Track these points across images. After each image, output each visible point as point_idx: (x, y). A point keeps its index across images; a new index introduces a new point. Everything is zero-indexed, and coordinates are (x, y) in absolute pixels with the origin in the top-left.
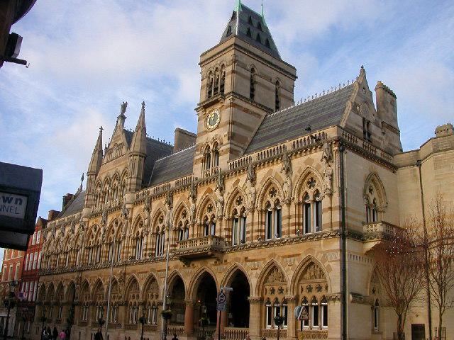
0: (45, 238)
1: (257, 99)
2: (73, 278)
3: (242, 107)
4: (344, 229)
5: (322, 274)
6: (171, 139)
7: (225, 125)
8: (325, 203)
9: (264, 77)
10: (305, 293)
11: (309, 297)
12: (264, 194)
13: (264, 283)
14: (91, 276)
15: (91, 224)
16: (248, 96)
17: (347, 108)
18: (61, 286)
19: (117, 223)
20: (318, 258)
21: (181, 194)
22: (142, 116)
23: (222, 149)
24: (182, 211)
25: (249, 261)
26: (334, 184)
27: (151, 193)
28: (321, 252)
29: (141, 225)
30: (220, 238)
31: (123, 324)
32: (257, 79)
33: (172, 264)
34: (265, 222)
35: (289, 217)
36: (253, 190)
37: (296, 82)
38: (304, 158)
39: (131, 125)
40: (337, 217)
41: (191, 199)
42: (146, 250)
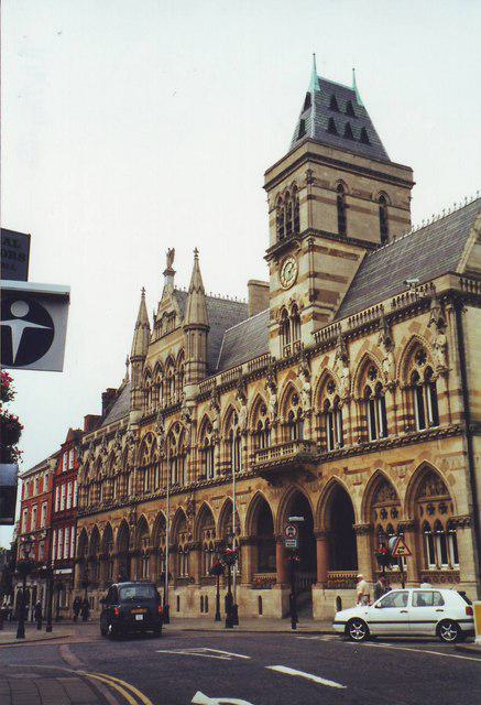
0: (80, 460)
1: (351, 233)
2: (125, 514)
3: (326, 249)
4: (468, 423)
5: (445, 489)
6: (242, 295)
7: (303, 280)
8: (441, 386)
9: (359, 195)
10: (426, 517)
11: (432, 521)
13: (373, 503)
14: (148, 511)
15: (143, 433)
16: (335, 230)
17: (469, 240)
18: (109, 530)
19: (178, 428)
20: (437, 465)
22: (197, 270)
23: (304, 314)
24: (259, 405)
25: (350, 473)
26: (450, 359)
27: (219, 383)
28: (440, 456)
29: (211, 429)
30: (309, 443)
31: (196, 577)
32: (349, 200)
33: (253, 483)
34: (366, 417)
35: (395, 408)
36: (346, 372)
37: (414, 192)
38: (408, 323)
39: (183, 282)
40: (457, 405)
41: (269, 389)
42: (219, 464)
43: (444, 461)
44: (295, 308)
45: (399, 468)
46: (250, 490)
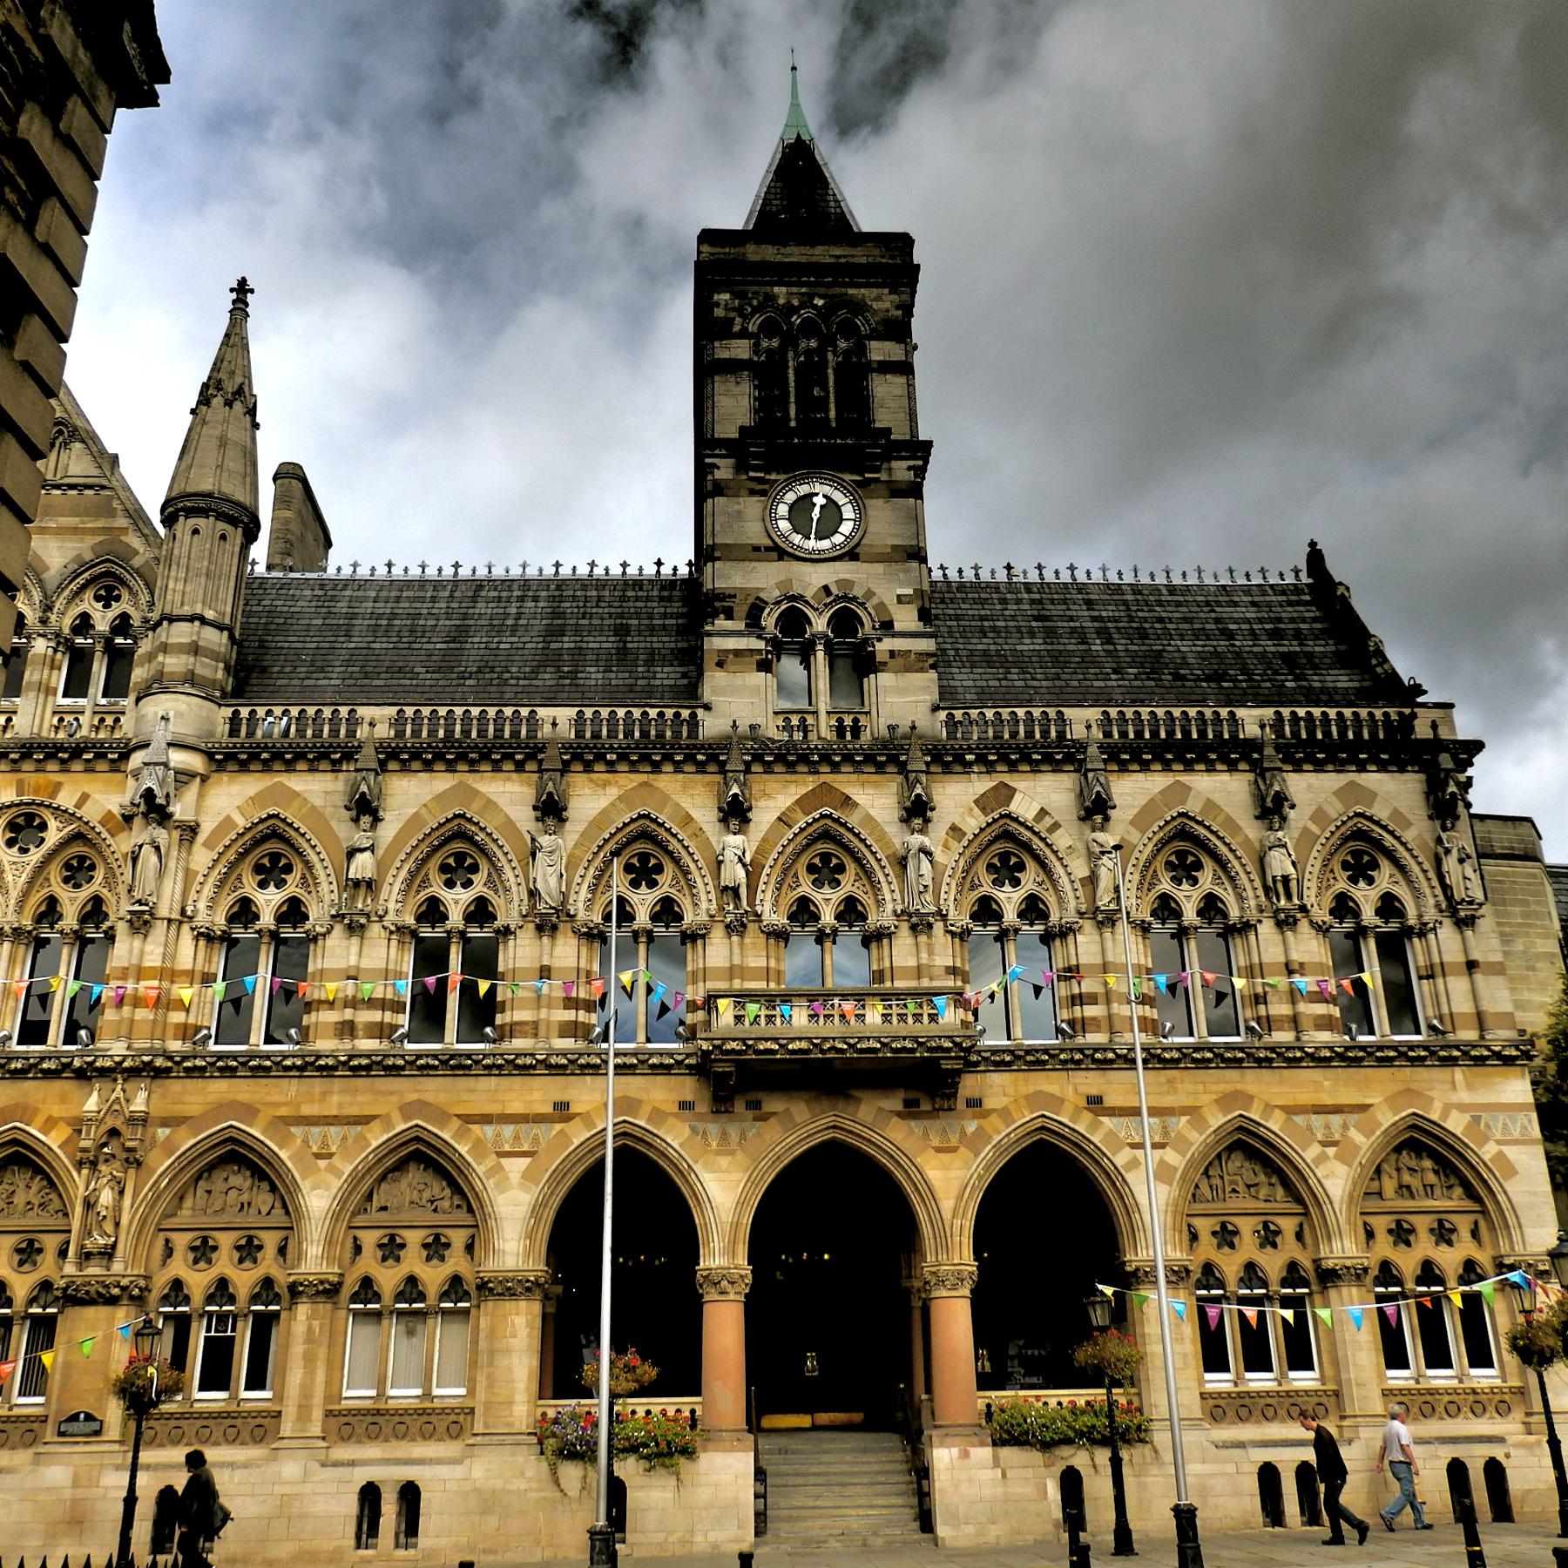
12: (1148, 864)
21: (628, 781)
28: (1462, 1108)
33: (584, 1093)
43: (1476, 1119)
44: (845, 621)
45: (1317, 1121)
46: (562, 1111)
